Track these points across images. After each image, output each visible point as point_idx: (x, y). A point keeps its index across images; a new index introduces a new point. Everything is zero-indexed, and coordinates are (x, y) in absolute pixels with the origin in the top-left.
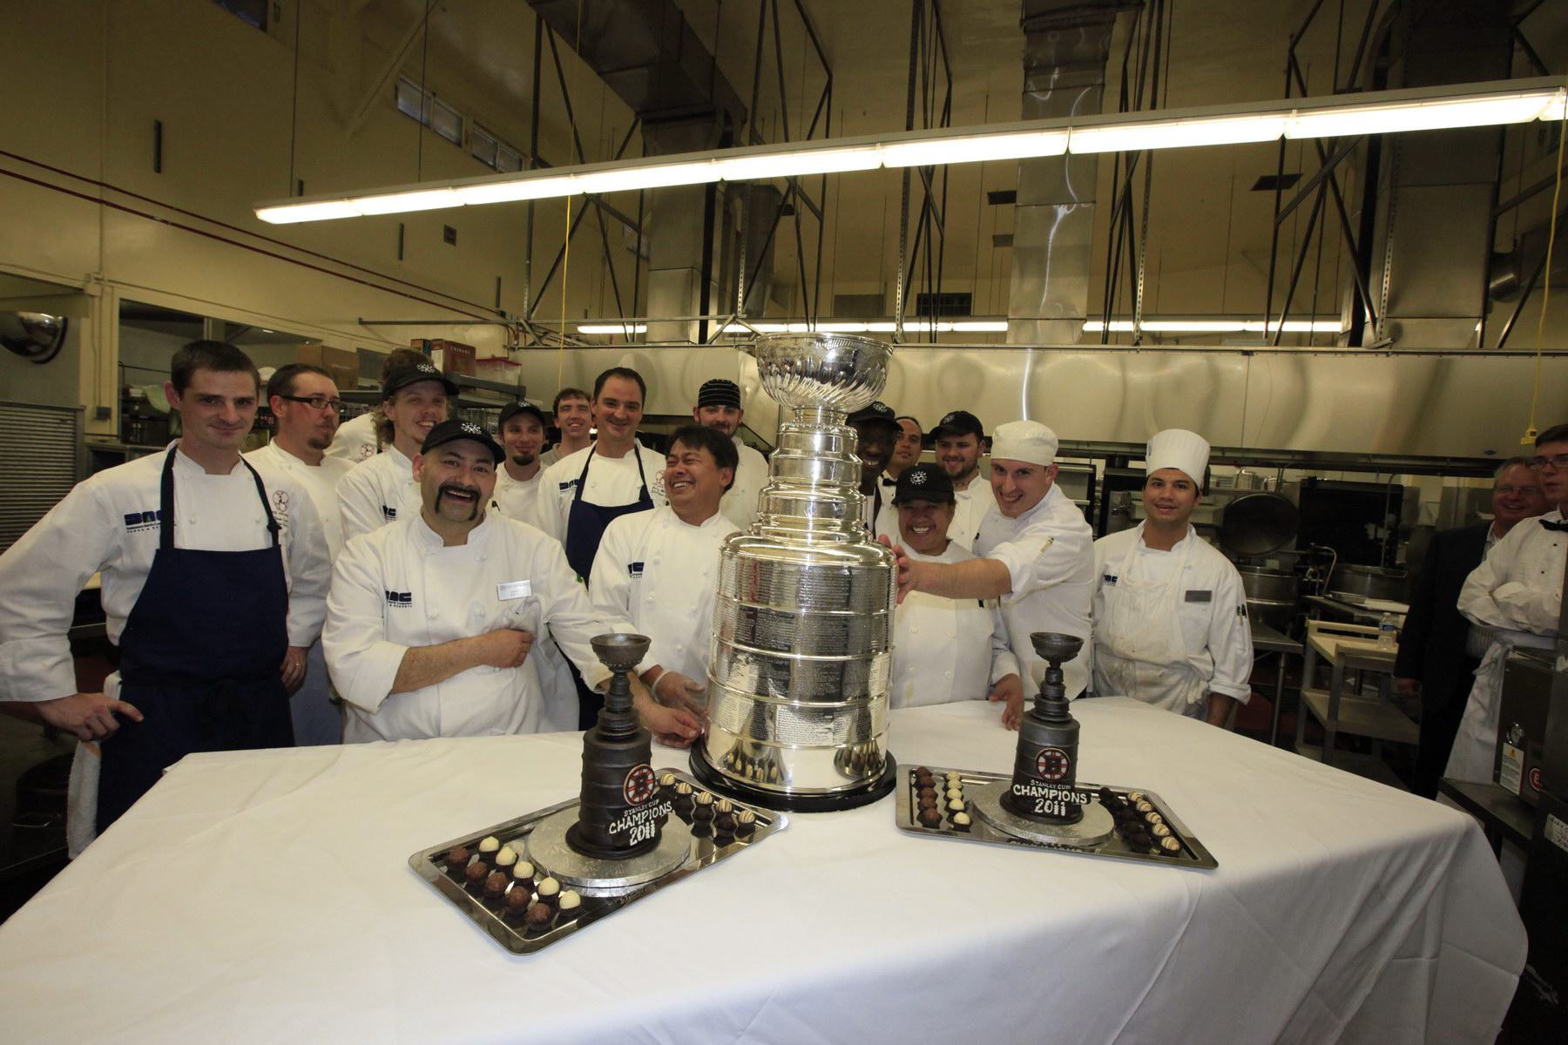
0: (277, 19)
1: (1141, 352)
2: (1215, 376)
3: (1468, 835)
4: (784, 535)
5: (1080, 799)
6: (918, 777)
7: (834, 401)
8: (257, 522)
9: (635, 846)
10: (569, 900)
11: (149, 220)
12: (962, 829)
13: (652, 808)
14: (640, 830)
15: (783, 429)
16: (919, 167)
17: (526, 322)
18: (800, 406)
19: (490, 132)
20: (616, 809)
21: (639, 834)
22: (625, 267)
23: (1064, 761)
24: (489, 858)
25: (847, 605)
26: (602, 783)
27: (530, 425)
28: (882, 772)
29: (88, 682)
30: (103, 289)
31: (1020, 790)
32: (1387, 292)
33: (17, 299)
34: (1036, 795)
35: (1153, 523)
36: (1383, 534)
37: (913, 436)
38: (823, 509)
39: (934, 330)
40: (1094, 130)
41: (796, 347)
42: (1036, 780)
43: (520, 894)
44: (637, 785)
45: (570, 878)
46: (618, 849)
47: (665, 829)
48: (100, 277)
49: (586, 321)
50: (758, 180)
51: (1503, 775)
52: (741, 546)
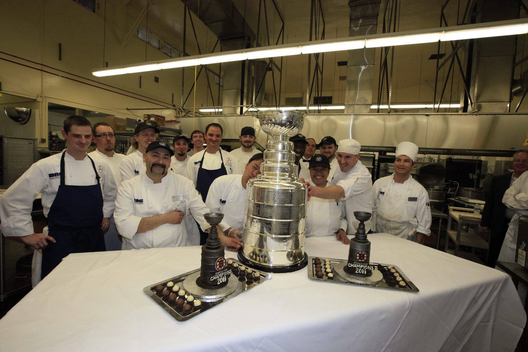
0: (99, 8)
1: (390, 116)
2: (416, 123)
3: (506, 281)
4: (269, 179)
5: (371, 268)
6: (315, 261)
7: (285, 133)
8: (92, 176)
9: (219, 284)
10: (197, 303)
11: (57, 76)
12: (330, 278)
13: (225, 272)
14: (221, 279)
15: (268, 143)
16: (314, 54)
17: (182, 108)
18: (274, 135)
19: (169, 44)
20: (213, 272)
22: (215, 88)
23: (365, 255)
24: (170, 289)
25: (291, 203)
26: (209, 263)
27: (183, 142)
28: (303, 259)
29: (38, 230)
30: (42, 100)
31: (350, 265)
32: (476, 93)
33: (15, 103)
34: (356, 267)
35: (397, 174)
36: (475, 177)
37: (313, 145)
38: (282, 169)
39: (319, 109)
40: (375, 39)
41: (272, 114)
42: (356, 262)
43: (180, 301)
44: (220, 264)
45: (197, 296)
46: (214, 286)
47: (229, 279)
48: (42, 95)
49: (202, 107)
50: (259, 59)
51: (518, 259)
52: (255, 182)
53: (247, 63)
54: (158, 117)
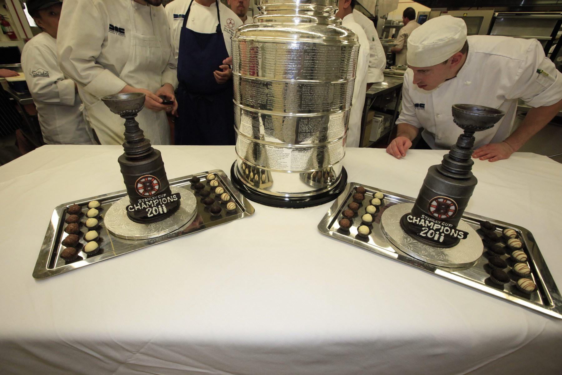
4: (271, 21)
5: (458, 234)
13: (161, 198)
21: (154, 212)
23: (453, 208)
31: (412, 219)
34: (424, 225)
42: (426, 215)
44: (145, 187)
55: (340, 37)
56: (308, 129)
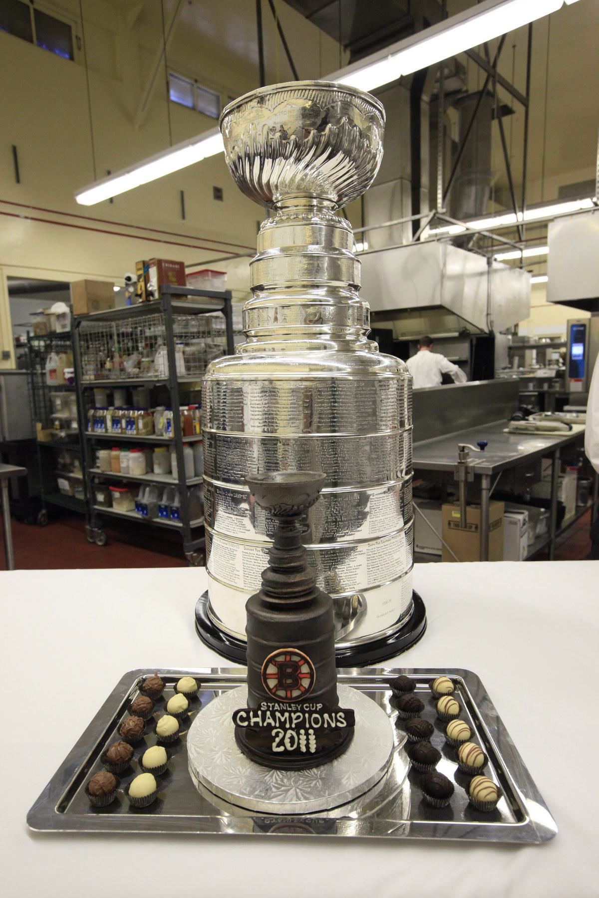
0: (79, 49)
11: (15, 218)
53: (425, 101)
54: (167, 265)
55: (377, 367)
56: (332, 516)
